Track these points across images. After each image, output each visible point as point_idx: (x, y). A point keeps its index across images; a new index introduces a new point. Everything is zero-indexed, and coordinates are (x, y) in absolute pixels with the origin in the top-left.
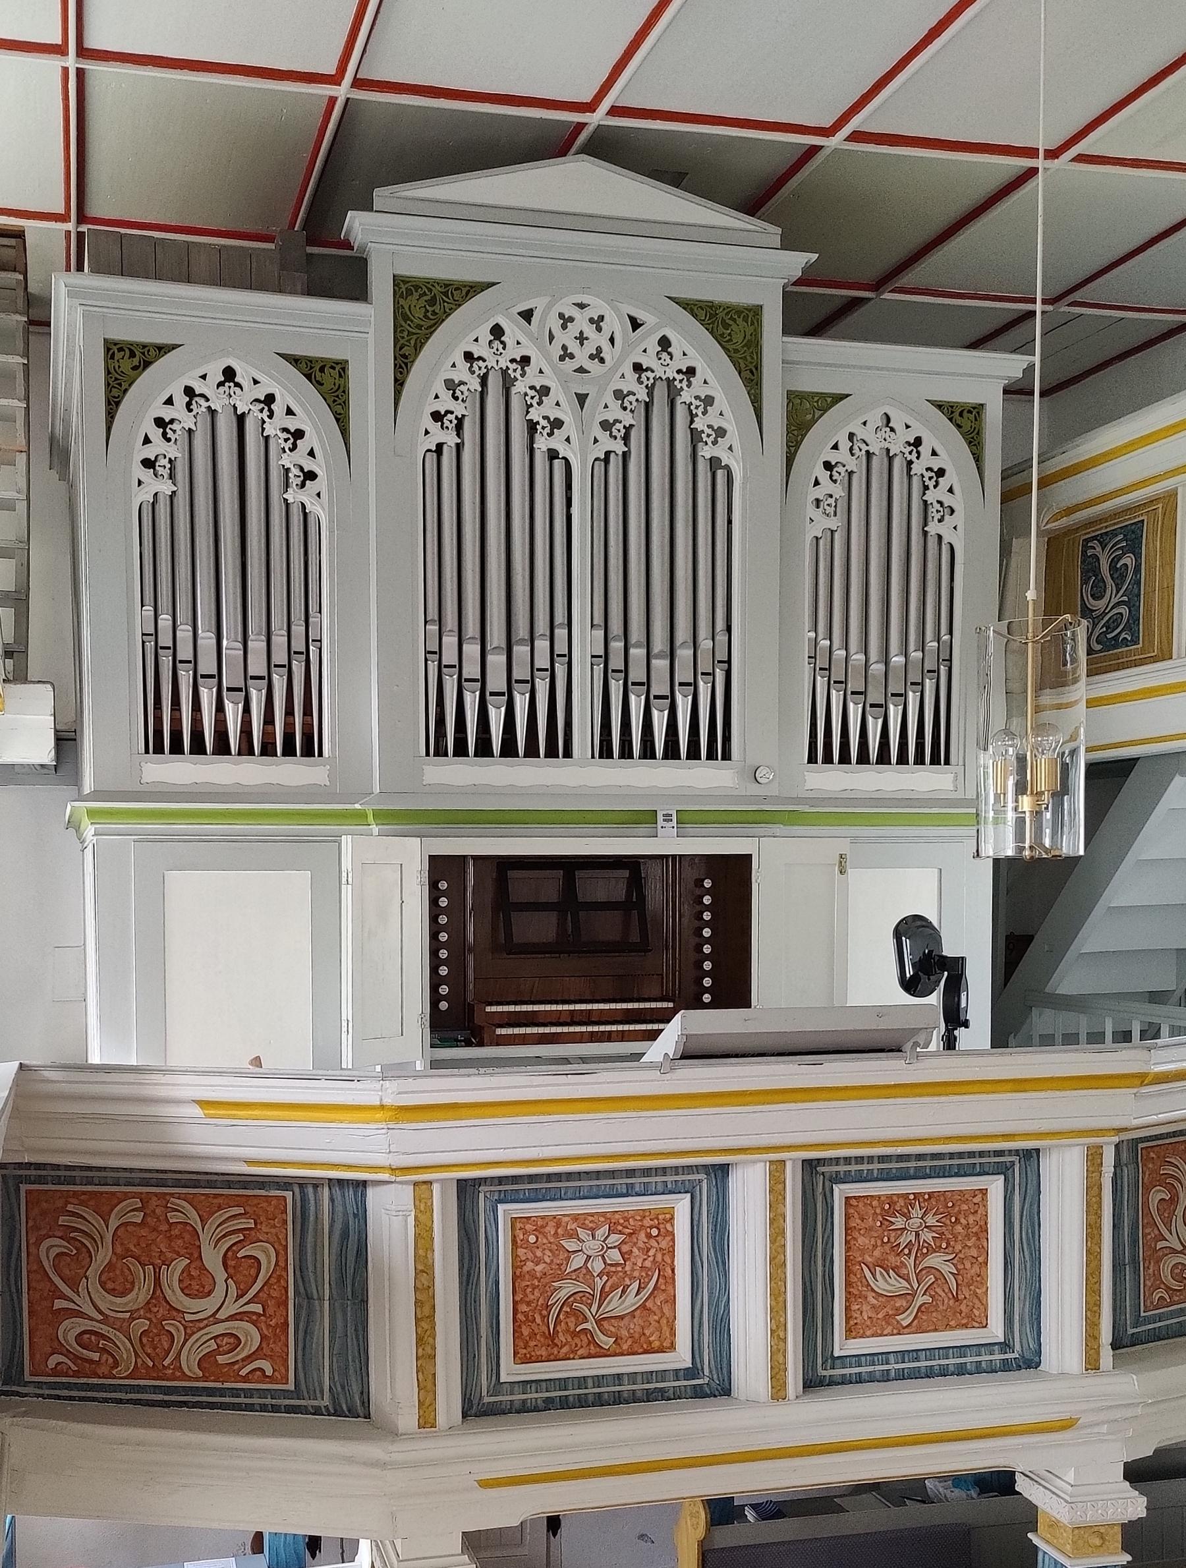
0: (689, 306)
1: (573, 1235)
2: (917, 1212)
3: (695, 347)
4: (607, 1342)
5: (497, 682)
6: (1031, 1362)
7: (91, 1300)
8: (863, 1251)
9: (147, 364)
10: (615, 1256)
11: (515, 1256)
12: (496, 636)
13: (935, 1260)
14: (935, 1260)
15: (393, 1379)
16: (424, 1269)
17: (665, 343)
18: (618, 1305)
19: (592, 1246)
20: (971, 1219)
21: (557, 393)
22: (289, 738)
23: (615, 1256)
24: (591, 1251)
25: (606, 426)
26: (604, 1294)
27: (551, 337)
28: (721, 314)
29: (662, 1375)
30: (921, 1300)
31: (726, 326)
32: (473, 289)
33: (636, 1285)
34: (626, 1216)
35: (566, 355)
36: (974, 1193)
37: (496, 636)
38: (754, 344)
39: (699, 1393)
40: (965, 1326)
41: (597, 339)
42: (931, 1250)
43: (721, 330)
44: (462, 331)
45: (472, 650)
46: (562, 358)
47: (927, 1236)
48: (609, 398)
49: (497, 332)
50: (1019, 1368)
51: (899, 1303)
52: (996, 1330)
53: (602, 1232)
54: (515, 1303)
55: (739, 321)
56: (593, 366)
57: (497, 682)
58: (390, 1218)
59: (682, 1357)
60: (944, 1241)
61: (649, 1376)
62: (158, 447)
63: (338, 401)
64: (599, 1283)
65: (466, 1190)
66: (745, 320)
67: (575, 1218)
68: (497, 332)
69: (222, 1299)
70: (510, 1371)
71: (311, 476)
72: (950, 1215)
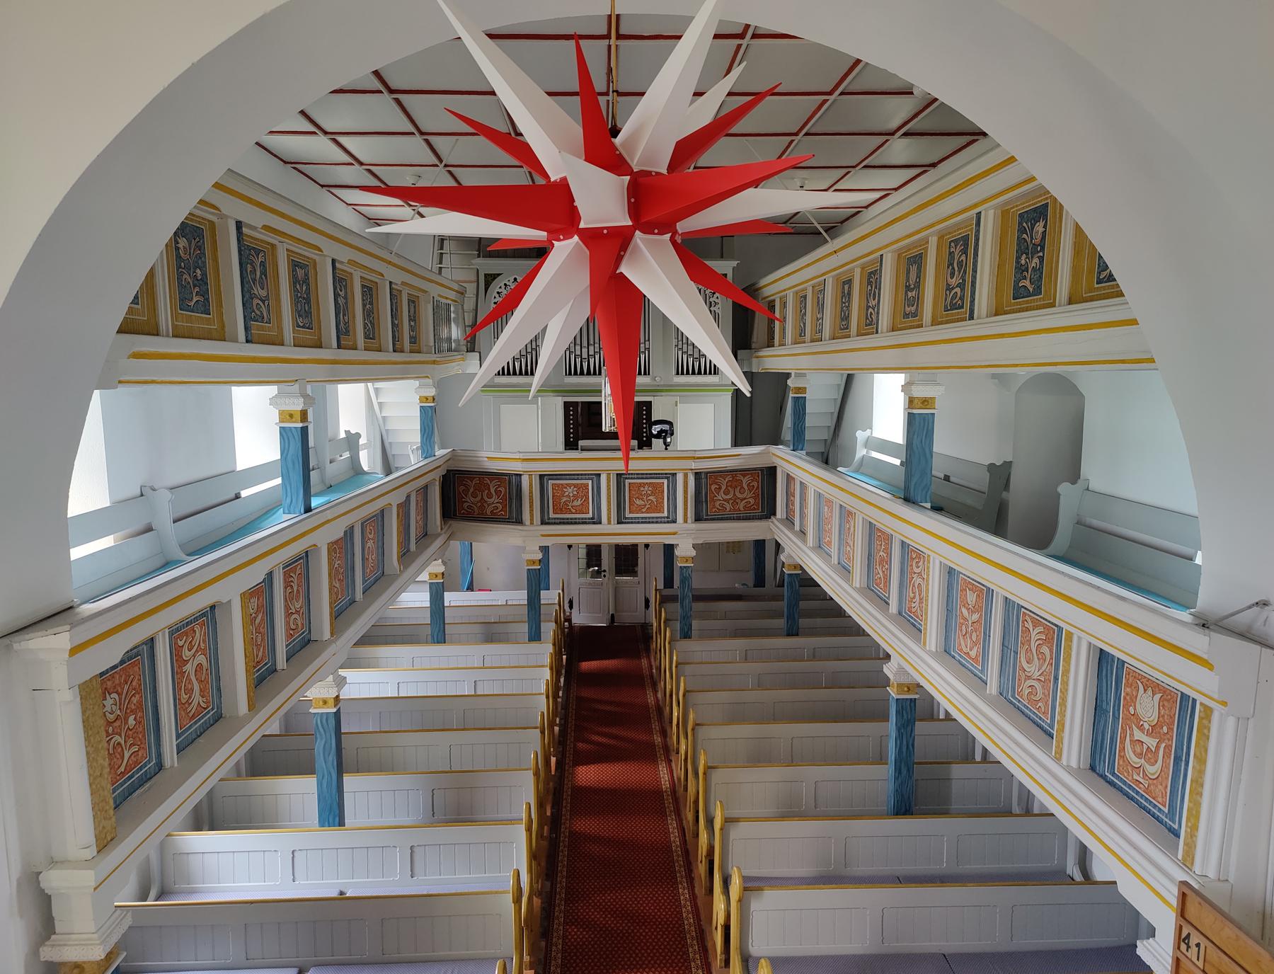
5: (585, 355)
6: (674, 521)
7: (470, 499)
12: (585, 344)
15: (526, 516)
16: (531, 492)
24: (570, 491)
37: (585, 344)
45: (578, 348)
52: (666, 514)
57: (585, 355)
58: (525, 481)
59: (590, 515)
65: (541, 477)
69: (494, 499)
70: (552, 515)
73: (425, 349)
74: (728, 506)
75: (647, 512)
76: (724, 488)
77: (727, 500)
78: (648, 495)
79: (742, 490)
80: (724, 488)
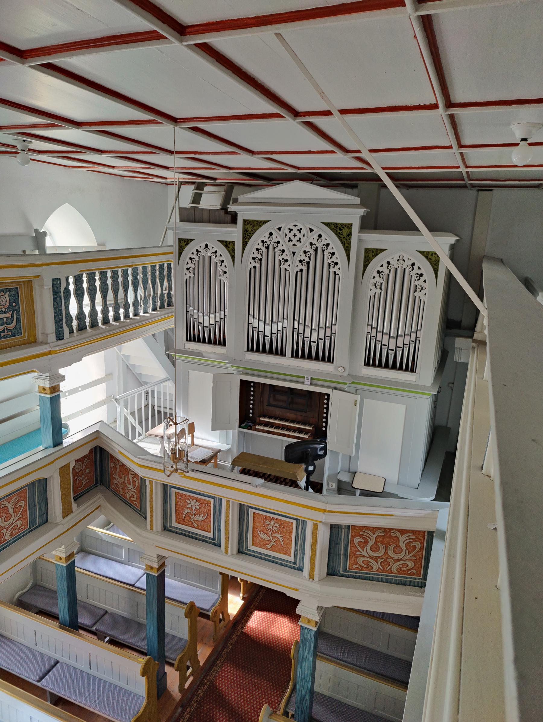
0: (328, 225)
1: (188, 499)
2: (273, 522)
3: (330, 237)
4: (196, 525)
8: (258, 526)
9: (188, 244)
10: (198, 507)
11: (176, 500)
13: (276, 535)
14: (277, 535)
17: (320, 236)
18: (197, 518)
19: (193, 503)
20: (288, 529)
21: (287, 252)
22: (220, 341)
23: (198, 507)
25: (301, 261)
26: (195, 515)
27: (286, 235)
28: (339, 226)
29: (206, 537)
30: (273, 543)
31: (341, 230)
32: (265, 222)
33: (202, 515)
34: (200, 499)
35: (290, 240)
36: (289, 522)
38: (349, 235)
39: (214, 544)
40: (285, 554)
41: (299, 235)
42: (276, 532)
43: (339, 231)
44: (260, 235)
46: (289, 241)
47: (276, 529)
48: (302, 253)
49: (271, 234)
50: (298, 570)
51: (267, 542)
53: (195, 501)
54: (176, 510)
55: (346, 228)
56: (298, 244)
59: (211, 535)
60: (279, 531)
61: (203, 536)
62: (190, 265)
63: (232, 253)
64: (194, 512)
66: (348, 227)
67: (189, 496)
68: (271, 234)
71: (225, 272)
72: (282, 525)
73: (40, 338)
74: (375, 566)
75: (272, 549)
76: (371, 543)
77: (375, 559)
78: (274, 532)
79: (397, 549)
80: (371, 543)
